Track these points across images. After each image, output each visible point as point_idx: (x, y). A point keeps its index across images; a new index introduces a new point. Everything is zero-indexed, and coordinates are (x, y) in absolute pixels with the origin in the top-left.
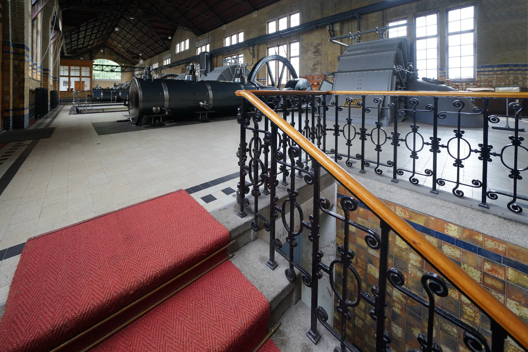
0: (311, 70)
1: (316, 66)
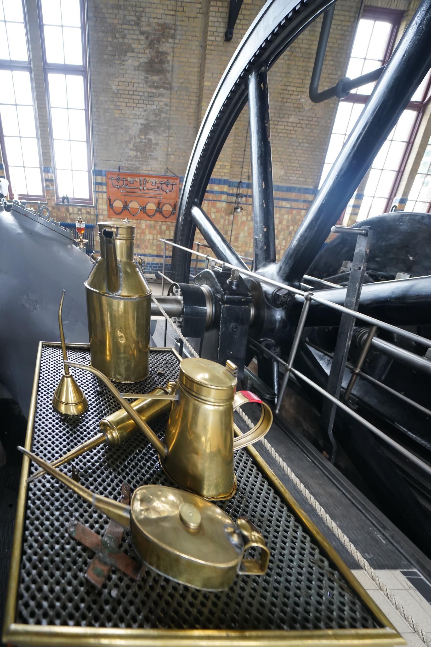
0: (136, 148)
1: (152, 136)
